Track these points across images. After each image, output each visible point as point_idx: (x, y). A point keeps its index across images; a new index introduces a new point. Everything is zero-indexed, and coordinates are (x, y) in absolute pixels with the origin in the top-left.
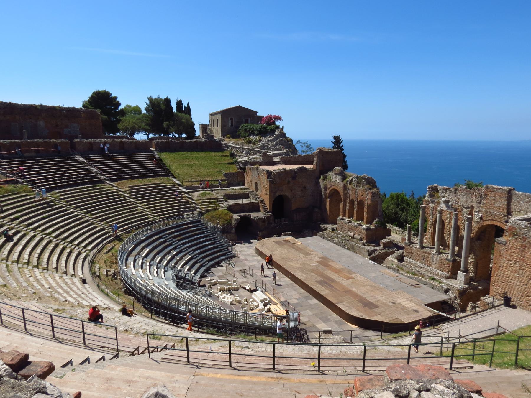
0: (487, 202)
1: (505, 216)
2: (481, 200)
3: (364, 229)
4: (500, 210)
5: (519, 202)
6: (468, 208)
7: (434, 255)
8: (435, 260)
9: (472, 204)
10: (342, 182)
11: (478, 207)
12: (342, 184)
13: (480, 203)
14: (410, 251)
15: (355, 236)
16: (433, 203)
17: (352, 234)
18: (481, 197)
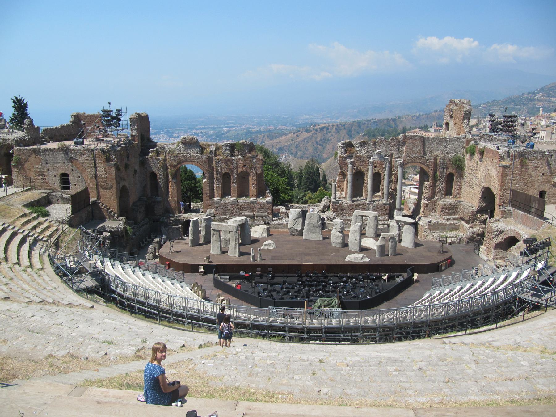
0: (406, 149)
4: (417, 153)
5: (430, 144)
10: (202, 153)
11: (397, 154)
13: (398, 150)
14: (340, 208)
16: (350, 159)
17: (251, 213)
18: (399, 145)
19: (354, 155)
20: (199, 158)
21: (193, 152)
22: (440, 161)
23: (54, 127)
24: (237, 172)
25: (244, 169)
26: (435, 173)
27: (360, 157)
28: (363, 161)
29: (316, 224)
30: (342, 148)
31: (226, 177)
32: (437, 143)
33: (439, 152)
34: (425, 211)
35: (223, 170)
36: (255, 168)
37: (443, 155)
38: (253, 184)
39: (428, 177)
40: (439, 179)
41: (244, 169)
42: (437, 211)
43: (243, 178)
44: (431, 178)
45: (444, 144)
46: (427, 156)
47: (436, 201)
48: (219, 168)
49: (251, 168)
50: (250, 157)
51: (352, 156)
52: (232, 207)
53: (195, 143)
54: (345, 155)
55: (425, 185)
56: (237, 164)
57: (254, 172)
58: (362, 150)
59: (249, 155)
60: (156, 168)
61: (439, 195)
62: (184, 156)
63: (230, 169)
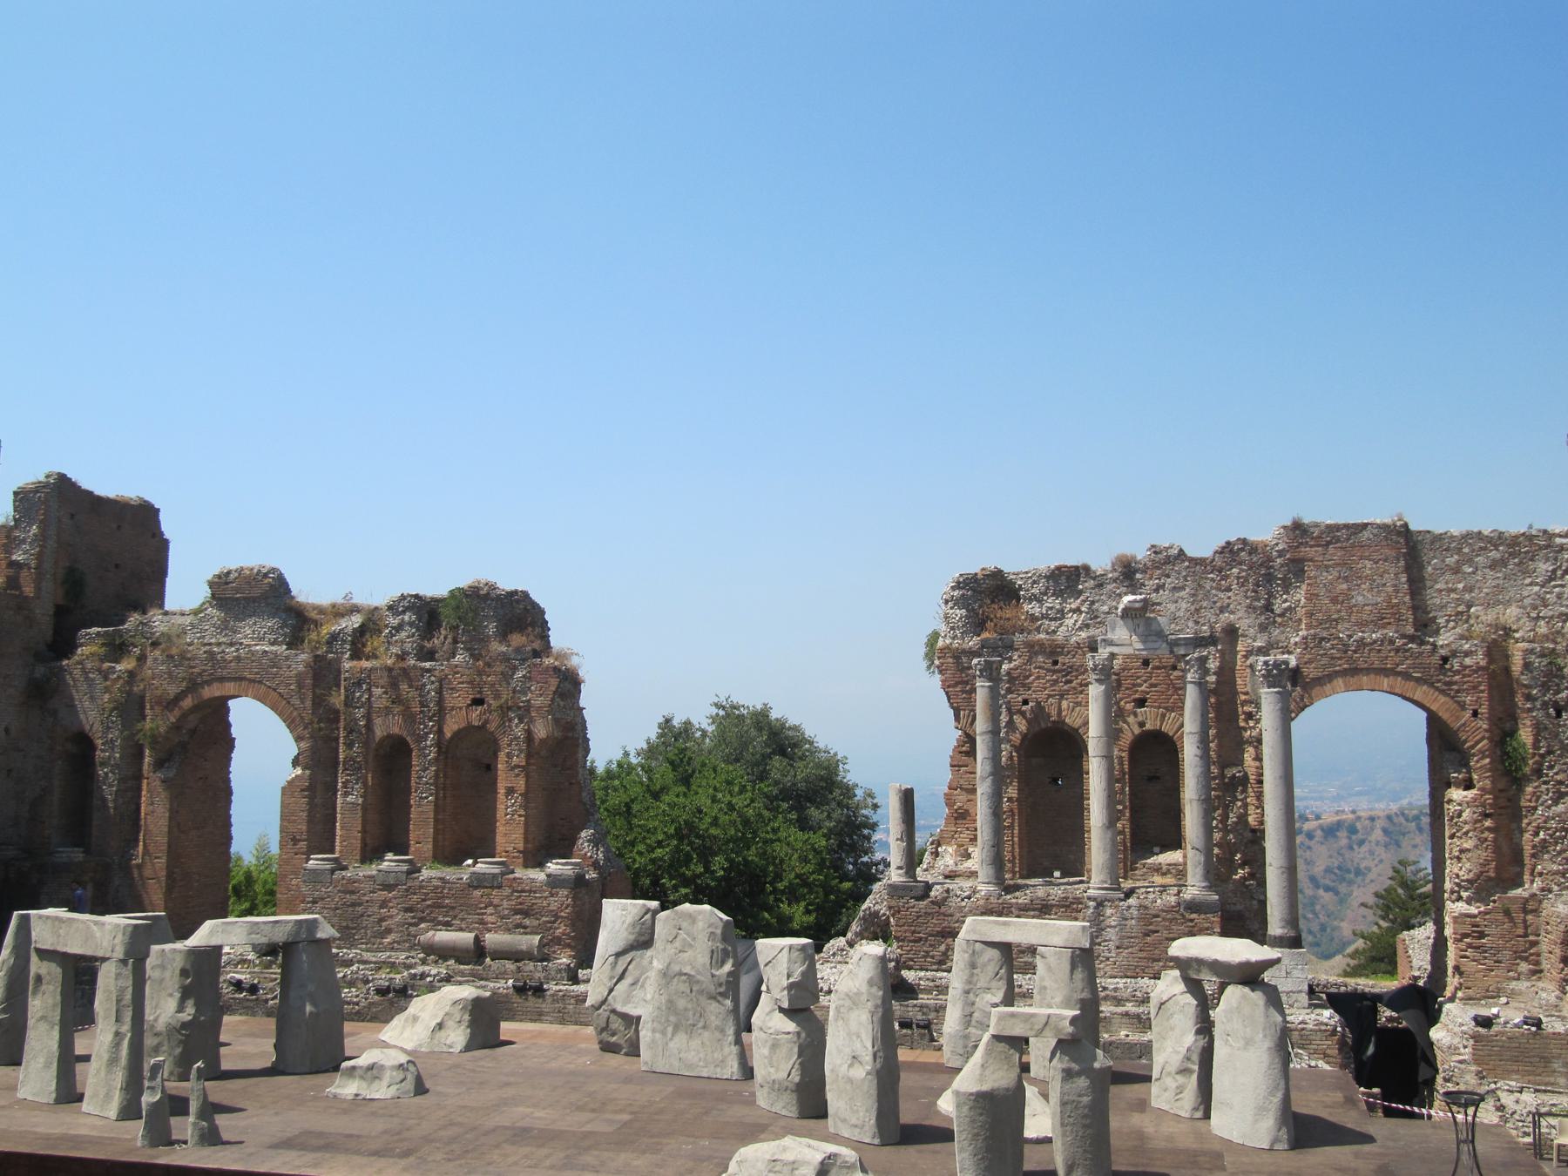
1: (1412, 639)
2: (1271, 595)
3: (554, 882)
4: (1379, 621)
5: (1456, 570)
6: (1211, 640)
7: (1100, 904)
8: (1111, 934)
9: (1226, 617)
10: (295, 642)
11: (1263, 628)
12: (301, 659)
13: (1268, 608)
14: (934, 924)
15: (491, 939)
17: (466, 938)
18: (1270, 578)
19: (1018, 638)
20: (275, 661)
21: (257, 637)
22: (1527, 666)
23: (234, 732)
24: (440, 732)
25: (475, 716)
26: (1503, 734)
27: (1053, 651)
28: (1069, 671)
29: (704, 978)
30: (957, 602)
31: (392, 760)
32: (1494, 566)
33: (1511, 614)
34: (1468, 966)
35: (378, 721)
36: (525, 712)
37: (1543, 628)
38: (510, 791)
39: (1463, 761)
40: (1538, 772)
41: (475, 716)
42: (1545, 965)
43: (470, 763)
44: (1480, 764)
45: (1544, 567)
46: (1444, 639)
47: (1531, 906)
48: (359, 713)
49: (504, 710)
50: (505, 658)
51: (1011, 647)
52: (384, 904)
53: (264, 597)
54: (973, 642)
55: (1452, 808)
56: (440, 692)
57: (519, 731)
58: (1061, 615)
59: (497, 647)
60: (92, 710)
61: (1547, 865)
62: (211, 654)
63: (409, 717)
